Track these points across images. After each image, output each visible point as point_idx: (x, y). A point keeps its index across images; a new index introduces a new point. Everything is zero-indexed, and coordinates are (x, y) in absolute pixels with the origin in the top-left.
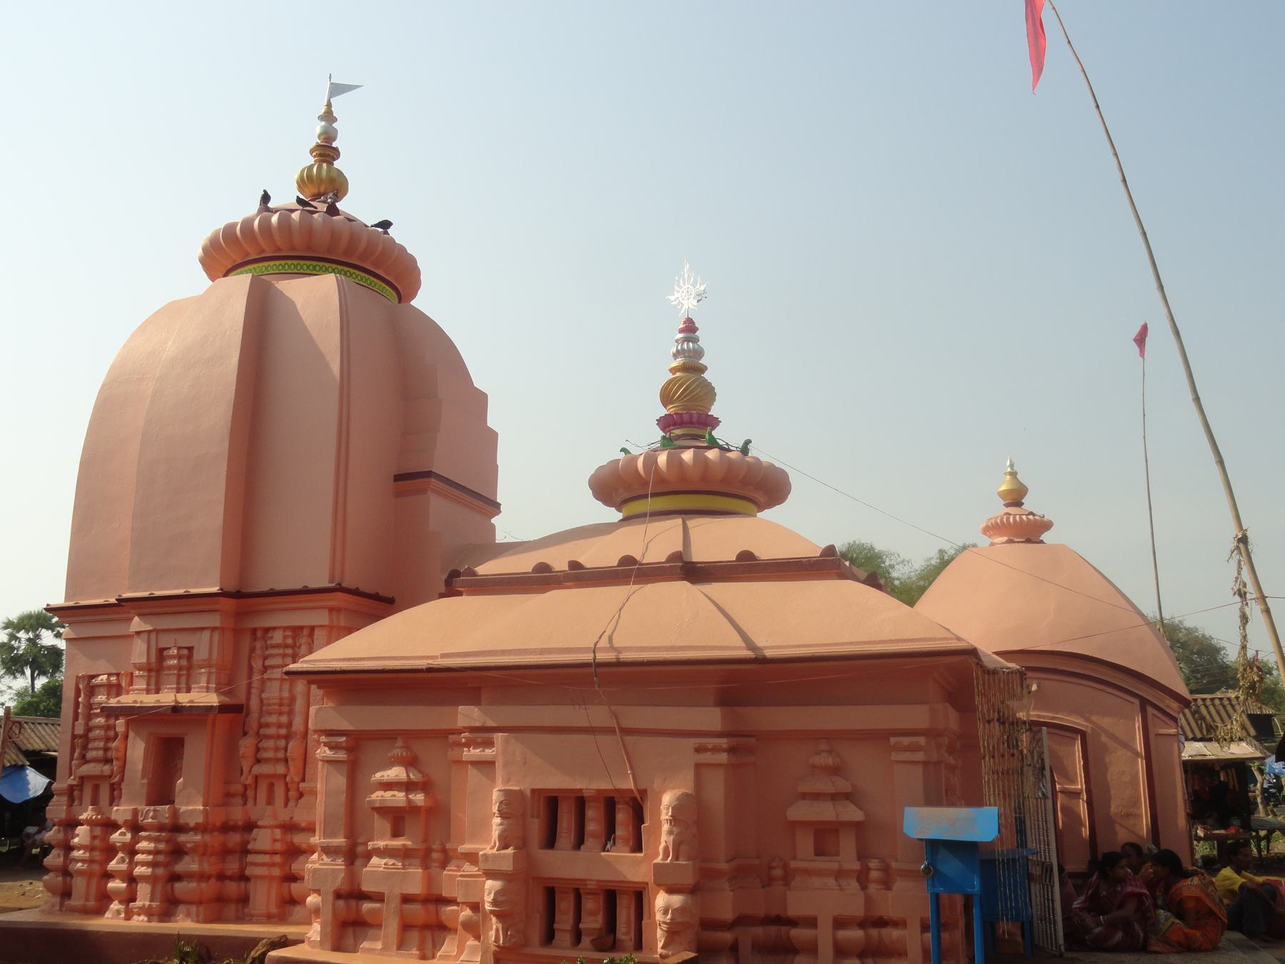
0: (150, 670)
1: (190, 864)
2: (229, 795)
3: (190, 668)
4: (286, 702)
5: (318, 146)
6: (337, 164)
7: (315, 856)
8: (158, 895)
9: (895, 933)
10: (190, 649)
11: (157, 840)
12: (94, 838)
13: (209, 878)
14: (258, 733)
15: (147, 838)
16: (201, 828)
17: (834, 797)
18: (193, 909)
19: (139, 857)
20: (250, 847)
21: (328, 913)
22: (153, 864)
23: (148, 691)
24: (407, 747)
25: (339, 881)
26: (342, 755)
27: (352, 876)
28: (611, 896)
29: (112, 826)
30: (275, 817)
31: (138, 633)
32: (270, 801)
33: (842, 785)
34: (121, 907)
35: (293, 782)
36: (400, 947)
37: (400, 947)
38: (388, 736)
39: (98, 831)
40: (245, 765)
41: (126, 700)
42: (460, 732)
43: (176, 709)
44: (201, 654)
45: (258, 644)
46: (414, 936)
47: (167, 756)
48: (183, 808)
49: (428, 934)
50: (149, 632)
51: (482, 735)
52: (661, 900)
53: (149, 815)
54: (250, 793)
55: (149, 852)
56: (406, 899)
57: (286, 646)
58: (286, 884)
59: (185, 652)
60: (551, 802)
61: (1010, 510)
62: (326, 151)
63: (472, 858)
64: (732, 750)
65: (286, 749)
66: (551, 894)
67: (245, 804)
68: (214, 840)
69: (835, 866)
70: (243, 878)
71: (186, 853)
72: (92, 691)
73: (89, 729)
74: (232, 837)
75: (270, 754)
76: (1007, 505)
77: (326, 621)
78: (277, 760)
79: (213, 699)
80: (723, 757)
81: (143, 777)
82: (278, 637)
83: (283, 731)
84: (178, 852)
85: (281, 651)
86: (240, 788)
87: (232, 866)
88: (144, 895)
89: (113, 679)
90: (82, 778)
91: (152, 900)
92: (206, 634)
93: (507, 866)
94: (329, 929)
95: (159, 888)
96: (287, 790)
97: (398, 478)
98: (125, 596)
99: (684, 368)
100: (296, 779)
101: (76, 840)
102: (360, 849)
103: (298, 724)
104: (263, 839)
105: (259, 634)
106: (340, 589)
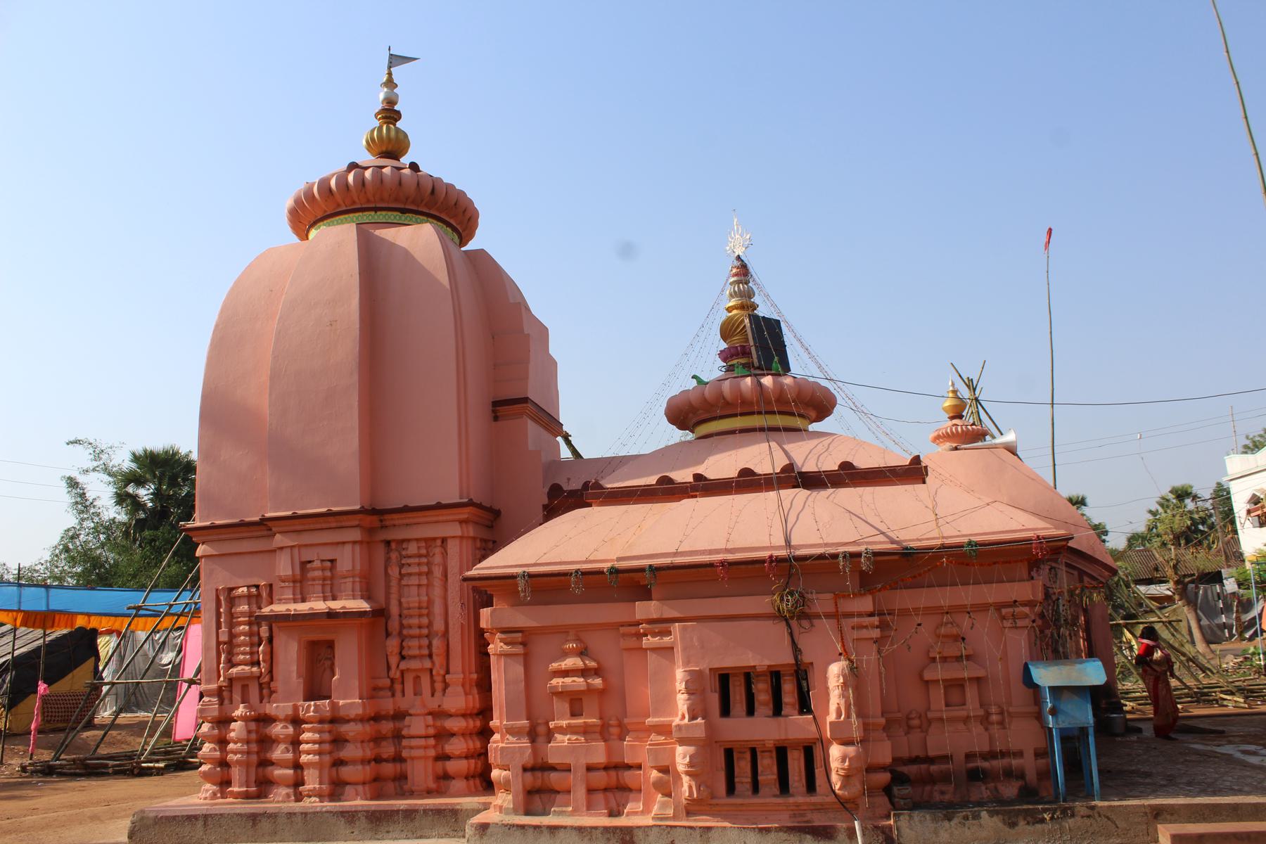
0: (294, 582)
1: (350, 752)
2: (376, 689)
3: (332, 578)
4: (425, 605)
5: (384, 110)
6: (399, 124)
7: (496, 737)
8: (326, 778)
9: (1015, 762)
10: (332, 561)
11: (320, 732)
12: (249, 732)
13: (369, 762)
14: (400, 633)
15: (309, 730)
16: (361, 719)
17: (959, 659)
18: (360, 788)
19: (304, 747)
20: (404, 732)
21: (518, 786)
22: (320, 753)
23: (295, 601)
24: (578, 640)
25: (527, 757)
26: (519, 649)
27: (535, 752)
28: (781, 753)
29: (267, 720)
30: (424, 706)
31: (282, 548)
32: (417, 693)
33: (963, 649)
34: (291, 791)
35: (438, 674)
36: (589, 808)
37: (589, 808)
38: (562, 631)
39: (253, 726)
40: (394, 660)
41: (279, 608)
42: (638, 624)
43: (331, 615)
44: (344, 565)
45: (394, 555)
46: (599, 797)
47: (319, 656)
48: (341, 702)
49: (610, 795)
50: (292, 547)
51: (661, 625)
52: (835, 751)
53: (310, 709)
54: (398, 687)
55: (314, 742)
56: (590, 768)
57: (420, 556)
58: (440, 764)
59: (329, 564)
60: (724, 679)
61: (955, 421)
62: (390, 114)
63: (664, 730)
64: (883, 626)
65: (430, 646)
66: (729, 753)
67: (393, 695)
68: (368, 728)
69: (964, 713)
70: (398, 759)
71: (347, 741)
72: (232, 601)
73: (232, 636)
74: (386, 725)
75: (416, 652)
76: (952, 418)
77: (459, 533)
78: (421, 657)
79: (363, 605)
80: (876, 633)
81: (299, 676)
82: (412, 548)
83: (425, 631)
84: (338, 741)
85: (417, 560)
86: (388, 682)
87: (388, 750)
88: (312, 781)
89: (253, 590)
90: (231, 680)
91: (321, 783)
92: (348, 548)
93: (700, 733)
94: (521, 797)
95: (326, 772)
96: (433, 682)
97: (496, 404)
98: (269, 515)
99: (742, 307)
100: (442, 672)
101: (233, 734)
102: (541, 729)
103: (439, 625)
104: (417, 725)
105: (393, 545)
106: (471, 503)
